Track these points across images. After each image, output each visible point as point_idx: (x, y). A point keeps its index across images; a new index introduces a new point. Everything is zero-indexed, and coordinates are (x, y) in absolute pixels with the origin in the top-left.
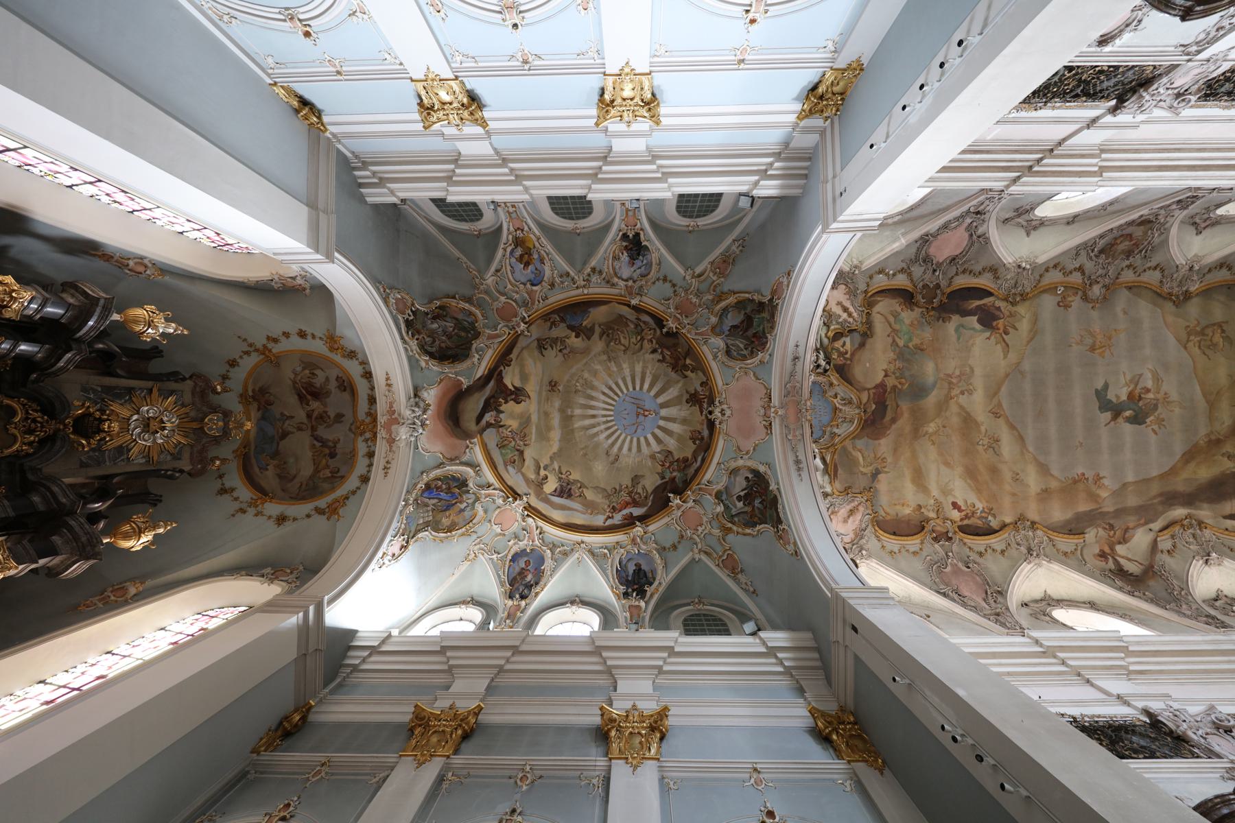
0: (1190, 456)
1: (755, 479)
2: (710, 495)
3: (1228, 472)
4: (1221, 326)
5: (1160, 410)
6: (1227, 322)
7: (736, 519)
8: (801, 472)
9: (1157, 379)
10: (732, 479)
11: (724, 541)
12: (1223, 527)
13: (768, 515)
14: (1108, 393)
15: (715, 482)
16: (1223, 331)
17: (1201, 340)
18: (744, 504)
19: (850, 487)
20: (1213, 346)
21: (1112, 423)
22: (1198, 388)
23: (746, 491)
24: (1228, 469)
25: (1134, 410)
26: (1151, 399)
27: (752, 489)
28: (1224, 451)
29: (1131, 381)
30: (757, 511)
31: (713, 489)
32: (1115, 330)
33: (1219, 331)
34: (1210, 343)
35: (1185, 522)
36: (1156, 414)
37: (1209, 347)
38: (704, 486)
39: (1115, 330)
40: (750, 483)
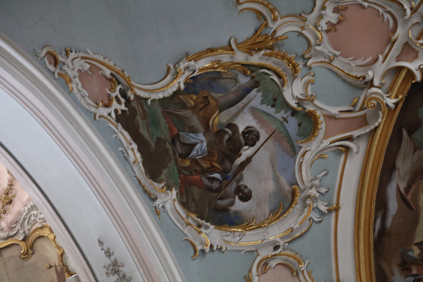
1: (223, 203)
2: (330, 117)
7: (244, 80)
8: (108, 261)
10: (283, 180)
11: (259, 14)
13: (163, 121)
15: (329, 155)
18: (233, 127)
19: (26, 255)
23: (239, 161)
27: (224, 172)
30: (195, 122)
31: (326, 137)
38: (355, 133)
40: (233, 186)
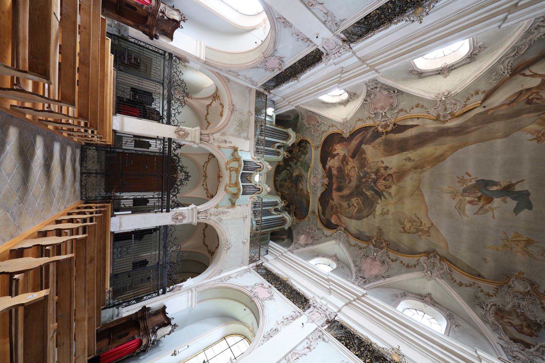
0: (440, 159)
3: (411, 151)
4: (404, 231)
5: (461, 189)
6: (400, 232)
9: (460, 209)
12: (420, 119)
14: (515, 205)
16: (403, 228)
17: (419, 227)
20: (411, 221)
21: (514, 182)
22: (426, 198)
24: (412, 152)
25: (488, 190)
26: (468, 196)
28: (412, 163)
29: (487, 211)
32: (498, 250)
33: (406, 229)
34: (413, 224)
35: (449, 117)
36: (465, 186)
37: (415, 221)
39: (498, 250)
